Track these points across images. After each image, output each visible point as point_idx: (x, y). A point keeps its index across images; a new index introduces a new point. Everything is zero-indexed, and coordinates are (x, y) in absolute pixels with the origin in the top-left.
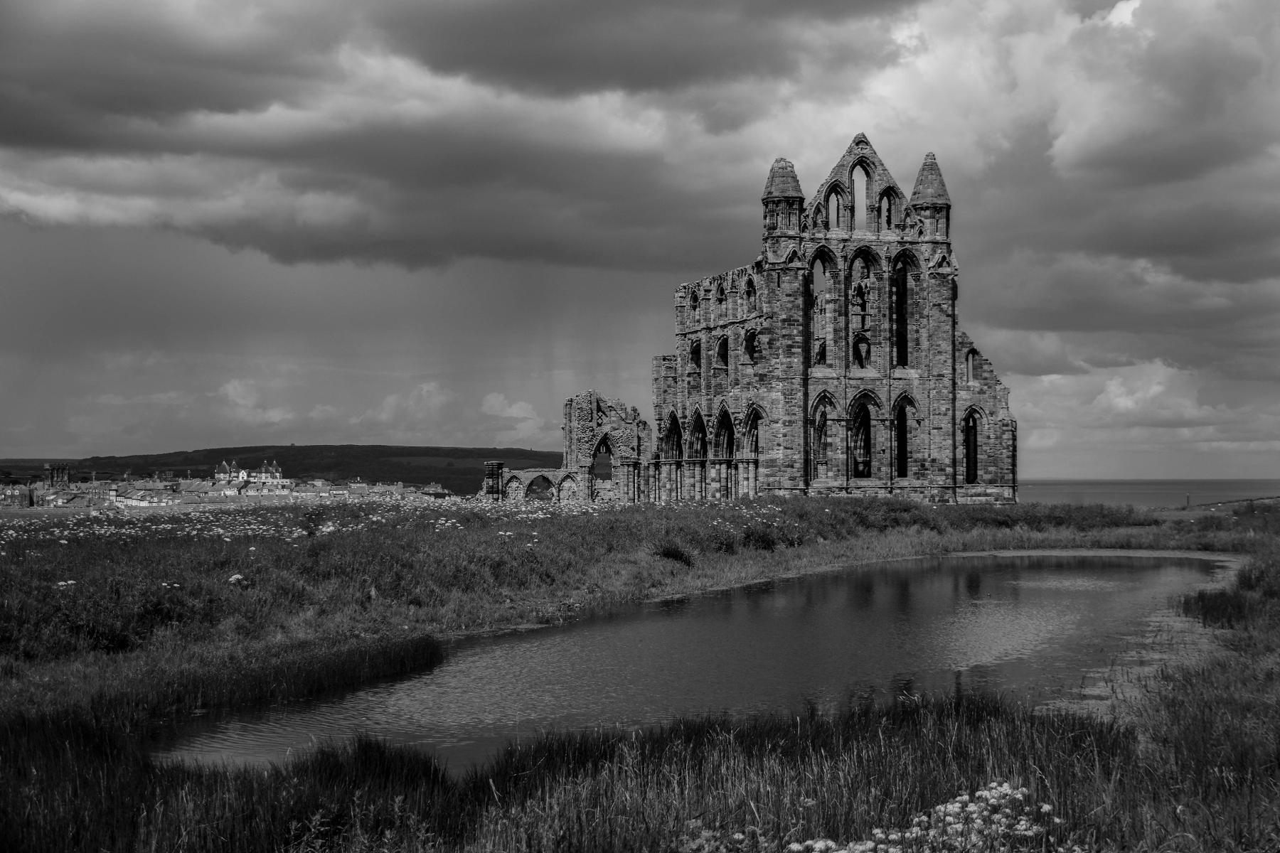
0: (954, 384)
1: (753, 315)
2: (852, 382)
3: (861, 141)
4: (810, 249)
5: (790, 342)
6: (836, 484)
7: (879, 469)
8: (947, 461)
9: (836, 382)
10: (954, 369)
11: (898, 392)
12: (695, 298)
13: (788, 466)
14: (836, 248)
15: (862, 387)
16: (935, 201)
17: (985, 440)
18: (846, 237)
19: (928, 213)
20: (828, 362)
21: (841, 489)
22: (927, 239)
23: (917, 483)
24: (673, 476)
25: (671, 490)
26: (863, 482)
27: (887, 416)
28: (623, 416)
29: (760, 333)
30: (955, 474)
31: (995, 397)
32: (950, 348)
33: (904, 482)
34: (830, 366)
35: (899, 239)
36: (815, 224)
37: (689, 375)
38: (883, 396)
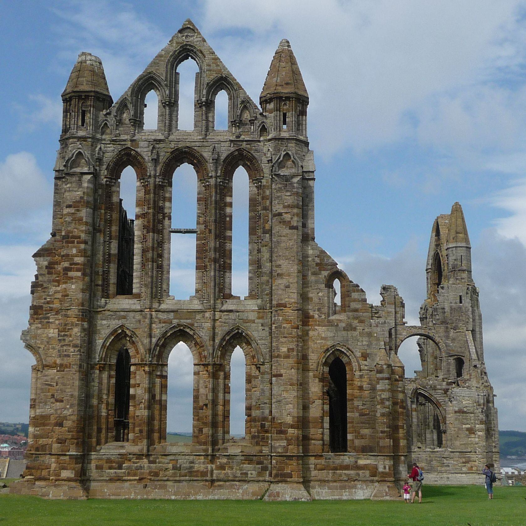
0: (305, 318)
2: (162, 316)
3: (188, 28)
4: (110, 152)
5: (66, 264)
6: (135, 449)
8: (289, 420)
9: (138, 316)
10: (304, 298)
11: (227, 329)
14: (144, 151)
15: (175, 322)
16: (280, 89)
17: (356, 392)
18: (162, 137)
19: (271, 106)
20: (134, 291)
21: (139, 456)
22: (270, 137)
27: (210, 360)
30: (306, 439)
31: (370, 335)
32: (294, 269)
34: (138, 296)
35: (233, 138)
36: (120, 122)
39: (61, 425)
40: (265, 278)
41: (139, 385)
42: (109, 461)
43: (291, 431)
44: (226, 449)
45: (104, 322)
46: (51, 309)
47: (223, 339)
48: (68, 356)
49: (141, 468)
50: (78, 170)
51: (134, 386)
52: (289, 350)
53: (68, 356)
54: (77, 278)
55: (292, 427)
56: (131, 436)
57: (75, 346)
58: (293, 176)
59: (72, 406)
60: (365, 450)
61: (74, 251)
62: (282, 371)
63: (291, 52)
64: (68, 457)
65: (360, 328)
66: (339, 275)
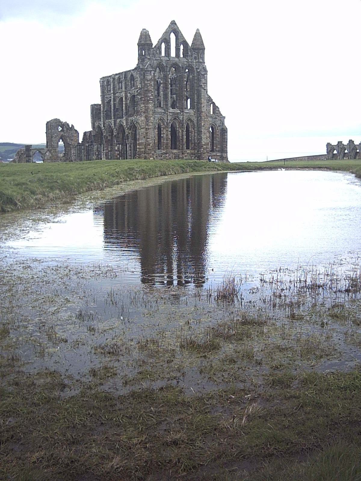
1: (133, 88)
3: (173, 23)
6: (164, 151)
7: (180, 146)
11: (186, 118)
12: (108, 82)
13: (148, 145)
18: (168, 59)
23: (193, 151)
24: (99, 150)
25: (98, 155)
26: (175, 151)
28: (68, 128)
29: (137, 95)
33: (188, 151)
37: (106, 111)
38: (181, 119)
39: (150, 145)
40: (196, 104)
41: (164, 134)
42: (159, 155)
43: (204, 146)
44: (186, 151)
45: (156, 116)
46: (142, 111)
47: (186, 121)
48: (150, 126)
49: (167, 156)
50: (150, 69)
51: (162, 134)
52: (204, 124)
53: (150, 126)
54: (152, 103)
55: (205, 145)
56: (162, 148)
57: (152, 123)
58: (205, 75)
59: (152, 140)
60: (218, 151)
61: (150, 95)
62: (202, 130)
63: (200, 33)
64: (151, 154)
65: (218, 119)
66: (214, 103)
